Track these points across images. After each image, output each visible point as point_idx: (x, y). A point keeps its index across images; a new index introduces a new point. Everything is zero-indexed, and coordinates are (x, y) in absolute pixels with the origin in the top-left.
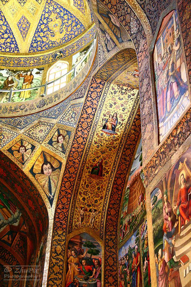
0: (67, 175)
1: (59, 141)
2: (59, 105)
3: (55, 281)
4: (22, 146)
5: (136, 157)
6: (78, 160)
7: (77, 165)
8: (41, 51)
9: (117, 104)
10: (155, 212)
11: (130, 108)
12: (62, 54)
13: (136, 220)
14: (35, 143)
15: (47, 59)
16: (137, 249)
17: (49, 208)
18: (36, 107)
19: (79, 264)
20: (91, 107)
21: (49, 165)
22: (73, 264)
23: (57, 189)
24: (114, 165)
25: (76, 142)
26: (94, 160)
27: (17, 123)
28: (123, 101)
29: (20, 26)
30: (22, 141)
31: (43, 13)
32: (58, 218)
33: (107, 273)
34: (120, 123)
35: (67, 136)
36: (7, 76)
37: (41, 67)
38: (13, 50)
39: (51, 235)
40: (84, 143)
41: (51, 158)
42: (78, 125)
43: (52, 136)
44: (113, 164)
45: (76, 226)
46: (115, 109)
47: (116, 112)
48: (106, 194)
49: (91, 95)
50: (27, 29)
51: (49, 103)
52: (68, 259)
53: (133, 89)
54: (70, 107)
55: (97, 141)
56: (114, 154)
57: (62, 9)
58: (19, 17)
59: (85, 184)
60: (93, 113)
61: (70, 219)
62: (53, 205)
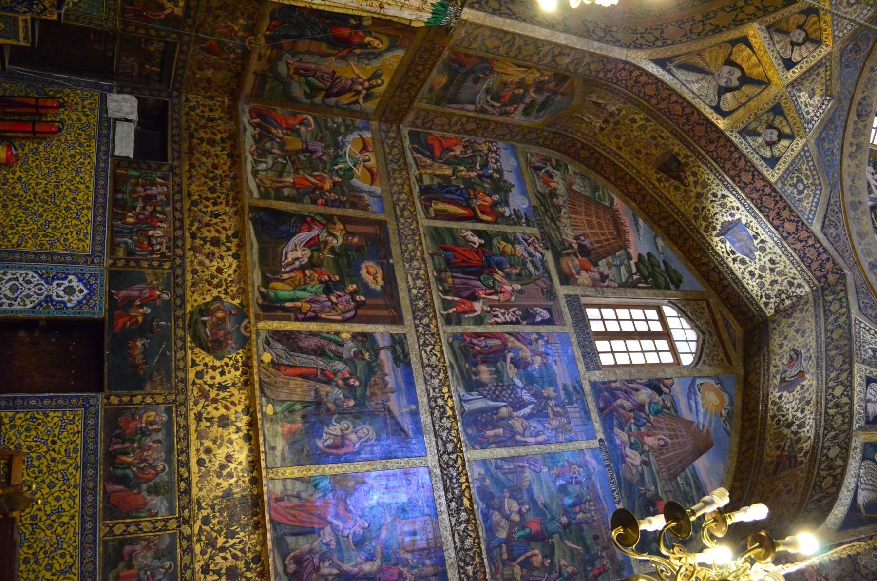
0: (695, 117)
4: (807, 39)
5: (660, 242)
7: (703, 143)
9: (768, 271)
11: (748, 284)
13: (553, 220)
14: (796, 72)
16: (502, 215)
17: (651, 55)
19: (521, 84)
21: (735, 83)
22: (523, 76)
23: (679, 84)
24: (666, 198)
25: (747, 168)
26: (694, 174)
27: (859, 43)
28: (767, 284)
32: (624, 69)
34: (733, 253)
35: (768, 154)
40: (737, 179)
41: (747, 96)
42: (777, 192)
43: (789, 118)
44: (669, 197)
45: (592, 92)
46: (762, 263)
47: (757, 260)
48: (621, 158)
51: (855, 129)
52: (538, 70)
53: (776, 311)
54: (820, 184)
55: (726, 201)
56: (686, 210)
59: (662, 138)
60: (781, 229)
62: (652, 65)
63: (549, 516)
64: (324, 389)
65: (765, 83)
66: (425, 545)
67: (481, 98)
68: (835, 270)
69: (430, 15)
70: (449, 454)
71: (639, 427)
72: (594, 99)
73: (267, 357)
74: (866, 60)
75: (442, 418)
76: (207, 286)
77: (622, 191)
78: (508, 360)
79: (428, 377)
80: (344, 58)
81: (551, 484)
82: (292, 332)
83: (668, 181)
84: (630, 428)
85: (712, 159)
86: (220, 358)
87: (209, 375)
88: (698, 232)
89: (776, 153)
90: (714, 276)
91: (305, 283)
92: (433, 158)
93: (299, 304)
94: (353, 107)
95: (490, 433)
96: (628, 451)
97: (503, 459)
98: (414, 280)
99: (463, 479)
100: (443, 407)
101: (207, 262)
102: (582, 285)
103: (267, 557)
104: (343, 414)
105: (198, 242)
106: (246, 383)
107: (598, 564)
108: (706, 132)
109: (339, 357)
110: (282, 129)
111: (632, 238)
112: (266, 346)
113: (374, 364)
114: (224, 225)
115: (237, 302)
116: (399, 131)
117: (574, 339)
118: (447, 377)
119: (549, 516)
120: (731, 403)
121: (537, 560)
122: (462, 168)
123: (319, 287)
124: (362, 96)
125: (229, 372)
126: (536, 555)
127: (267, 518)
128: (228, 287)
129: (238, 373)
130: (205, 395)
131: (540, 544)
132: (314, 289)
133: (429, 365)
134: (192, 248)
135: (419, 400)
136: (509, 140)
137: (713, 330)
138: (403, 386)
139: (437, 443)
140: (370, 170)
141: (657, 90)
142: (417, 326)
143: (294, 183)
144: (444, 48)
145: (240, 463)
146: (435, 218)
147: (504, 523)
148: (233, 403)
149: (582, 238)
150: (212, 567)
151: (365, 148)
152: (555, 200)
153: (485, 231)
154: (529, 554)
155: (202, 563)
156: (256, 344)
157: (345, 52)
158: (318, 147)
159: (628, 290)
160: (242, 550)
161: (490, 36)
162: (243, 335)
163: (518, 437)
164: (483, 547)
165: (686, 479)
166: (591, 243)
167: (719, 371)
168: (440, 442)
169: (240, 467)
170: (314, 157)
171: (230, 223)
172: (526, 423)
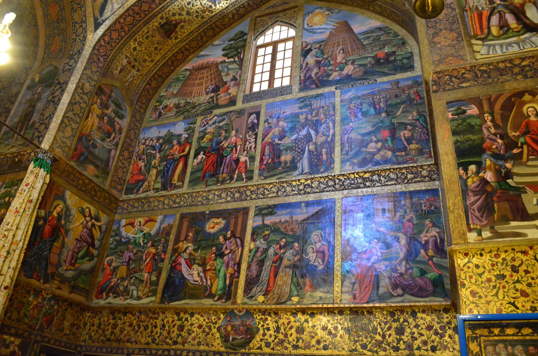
0: (136, 9)
3: (71, 123)
5: (216, 43)
7: (153, 6)
10: (459, 125)
13: (194, 107)
16: (187, 139)
17: (91, 32)
19: (101, 117)
24: (188, 35)
26: (174, 15)
32: (98, 50)
33: (125, 144)
39: (84, 65)
45: (112, 73)
48: (158, 61)
52: (92, 105)
59: (148, 32)
61: (109, 62)
62: (98, 31)
63: (381, 124)
64: (285, 262)
66: (392, 203)
67: (107, 144)
69: (42, 170)
70: (335, 184)
71: (330, 65)
72: (117, 72)
73: (261, 298)
75: (312, 187)
76: (210, 336)
77: (181, 63)
78: (279, 142)
79: (285, 194)
80: (67, 232)
81: (361, 121)
82: (246, 281)
83: (177, 32)
84: (331, 70)
86: (258, 329)
87: (269, 338)
88: (212, 17)
90: (242, 11)
91: (215, 270)
92: (144, 181)
93: (228, 275)
94: (103, 229)
95: (324, 157)
96: (345, 72)
97: (342, 150)
98: (221, 199)
99: (352, 176)
100: (305, 186)
101: (193, 335)
102: (237, 92)
103: (391, 307)
104: (303, 251)
105: (180, 340)
106: (276, 314)
107: (413, 96)
109: (266, 250)
110: (112, 278)
111: (211, 59)
112: (254, 298)
113: (273, 228)
114: (170, 321)
115: (222, 316)
116: (123, 201)
117: (271, 100)
118: (286, 182)
119: (381, 124)
120: (322, 8)
121: (407, 134)
122: (153, 162)
123: (219, 261)
124: (96, 223)
125: (268, 324)
126: (404, 134)
127: (365, 305)
128: (212, 322)
129: (269, 318)
130: (282, 342)
131: (397, 131)
132: (220, 264)
133: (277, 193)
134: (183, 344)
135: (298, 200)
136: (139, 131)
137: (275, 16)
138: (289, 210)
139: (327, 191)
140: (147, 222)
141: (115, 30)
142: (251, 199)
143: (149, 273)
144: (68, 164)
145: (329, 321)
146: (183, 182)
147: (382, 153)
148: (288, 323)
149: (208, 90)
150: (395, 344)
151: (132, 224)
152: (182, 105)
153: (196, 151)
154: (403, 138)
155: (392, 351)
156: (251, 304)
157: (63, 231)
158: (127, 255)
159: (244, 64)
160: (386, 323)
161: (63, 132)
162: (245, 314)
163: (329, 139)
164: (396, 167)
165: (365, 39)
166: (212, 85)
167: (301, 13)
168: (327, 189)
169: (331, 322)
170: (133, 258)
171: (170, 317)
172: (320, 134)
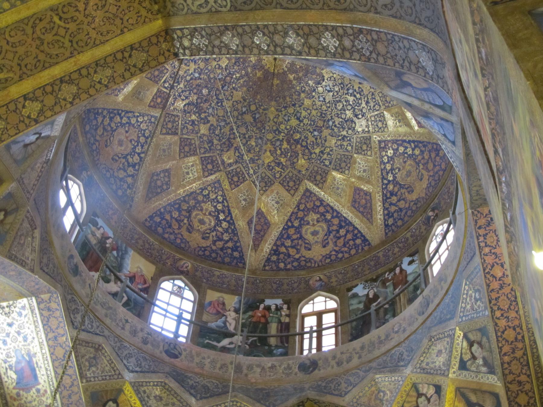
1: (476, 355)
2: (450, 292)
4: (420, 395)
6: (525, 374)
7: (527, 387)
8: (403, 225)
12: (436, 211)
14: (438, 380)
15: (418, 231)
18: (417, 316)
20: (497, 264)
25: (504, 342)
27: (397, 360)
29: (357, 206)
30: (415, 386)
31: (383, 167)
35: (484, 339)
36: (366, 292)
37: (413, 249)
38: (360, 248)
40: (519, 337)
41: (475, 394)
42: (491, 308)
43: (459, 352)
49: (486, 243)
50: (369, 205)
51: (435, 296)
54: (466, 284)
57: (405, 144)
58: (349, 192)
65: (459, 391)
68: (479, 215)
74: (402, 342)
85: (529, 368)
89: (479, 334)
108: (518, 394)
